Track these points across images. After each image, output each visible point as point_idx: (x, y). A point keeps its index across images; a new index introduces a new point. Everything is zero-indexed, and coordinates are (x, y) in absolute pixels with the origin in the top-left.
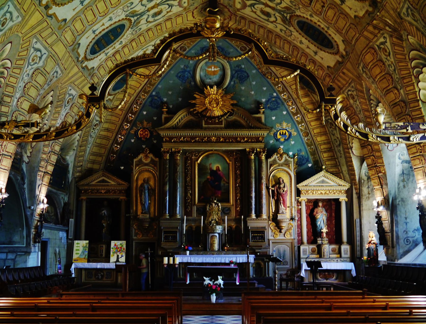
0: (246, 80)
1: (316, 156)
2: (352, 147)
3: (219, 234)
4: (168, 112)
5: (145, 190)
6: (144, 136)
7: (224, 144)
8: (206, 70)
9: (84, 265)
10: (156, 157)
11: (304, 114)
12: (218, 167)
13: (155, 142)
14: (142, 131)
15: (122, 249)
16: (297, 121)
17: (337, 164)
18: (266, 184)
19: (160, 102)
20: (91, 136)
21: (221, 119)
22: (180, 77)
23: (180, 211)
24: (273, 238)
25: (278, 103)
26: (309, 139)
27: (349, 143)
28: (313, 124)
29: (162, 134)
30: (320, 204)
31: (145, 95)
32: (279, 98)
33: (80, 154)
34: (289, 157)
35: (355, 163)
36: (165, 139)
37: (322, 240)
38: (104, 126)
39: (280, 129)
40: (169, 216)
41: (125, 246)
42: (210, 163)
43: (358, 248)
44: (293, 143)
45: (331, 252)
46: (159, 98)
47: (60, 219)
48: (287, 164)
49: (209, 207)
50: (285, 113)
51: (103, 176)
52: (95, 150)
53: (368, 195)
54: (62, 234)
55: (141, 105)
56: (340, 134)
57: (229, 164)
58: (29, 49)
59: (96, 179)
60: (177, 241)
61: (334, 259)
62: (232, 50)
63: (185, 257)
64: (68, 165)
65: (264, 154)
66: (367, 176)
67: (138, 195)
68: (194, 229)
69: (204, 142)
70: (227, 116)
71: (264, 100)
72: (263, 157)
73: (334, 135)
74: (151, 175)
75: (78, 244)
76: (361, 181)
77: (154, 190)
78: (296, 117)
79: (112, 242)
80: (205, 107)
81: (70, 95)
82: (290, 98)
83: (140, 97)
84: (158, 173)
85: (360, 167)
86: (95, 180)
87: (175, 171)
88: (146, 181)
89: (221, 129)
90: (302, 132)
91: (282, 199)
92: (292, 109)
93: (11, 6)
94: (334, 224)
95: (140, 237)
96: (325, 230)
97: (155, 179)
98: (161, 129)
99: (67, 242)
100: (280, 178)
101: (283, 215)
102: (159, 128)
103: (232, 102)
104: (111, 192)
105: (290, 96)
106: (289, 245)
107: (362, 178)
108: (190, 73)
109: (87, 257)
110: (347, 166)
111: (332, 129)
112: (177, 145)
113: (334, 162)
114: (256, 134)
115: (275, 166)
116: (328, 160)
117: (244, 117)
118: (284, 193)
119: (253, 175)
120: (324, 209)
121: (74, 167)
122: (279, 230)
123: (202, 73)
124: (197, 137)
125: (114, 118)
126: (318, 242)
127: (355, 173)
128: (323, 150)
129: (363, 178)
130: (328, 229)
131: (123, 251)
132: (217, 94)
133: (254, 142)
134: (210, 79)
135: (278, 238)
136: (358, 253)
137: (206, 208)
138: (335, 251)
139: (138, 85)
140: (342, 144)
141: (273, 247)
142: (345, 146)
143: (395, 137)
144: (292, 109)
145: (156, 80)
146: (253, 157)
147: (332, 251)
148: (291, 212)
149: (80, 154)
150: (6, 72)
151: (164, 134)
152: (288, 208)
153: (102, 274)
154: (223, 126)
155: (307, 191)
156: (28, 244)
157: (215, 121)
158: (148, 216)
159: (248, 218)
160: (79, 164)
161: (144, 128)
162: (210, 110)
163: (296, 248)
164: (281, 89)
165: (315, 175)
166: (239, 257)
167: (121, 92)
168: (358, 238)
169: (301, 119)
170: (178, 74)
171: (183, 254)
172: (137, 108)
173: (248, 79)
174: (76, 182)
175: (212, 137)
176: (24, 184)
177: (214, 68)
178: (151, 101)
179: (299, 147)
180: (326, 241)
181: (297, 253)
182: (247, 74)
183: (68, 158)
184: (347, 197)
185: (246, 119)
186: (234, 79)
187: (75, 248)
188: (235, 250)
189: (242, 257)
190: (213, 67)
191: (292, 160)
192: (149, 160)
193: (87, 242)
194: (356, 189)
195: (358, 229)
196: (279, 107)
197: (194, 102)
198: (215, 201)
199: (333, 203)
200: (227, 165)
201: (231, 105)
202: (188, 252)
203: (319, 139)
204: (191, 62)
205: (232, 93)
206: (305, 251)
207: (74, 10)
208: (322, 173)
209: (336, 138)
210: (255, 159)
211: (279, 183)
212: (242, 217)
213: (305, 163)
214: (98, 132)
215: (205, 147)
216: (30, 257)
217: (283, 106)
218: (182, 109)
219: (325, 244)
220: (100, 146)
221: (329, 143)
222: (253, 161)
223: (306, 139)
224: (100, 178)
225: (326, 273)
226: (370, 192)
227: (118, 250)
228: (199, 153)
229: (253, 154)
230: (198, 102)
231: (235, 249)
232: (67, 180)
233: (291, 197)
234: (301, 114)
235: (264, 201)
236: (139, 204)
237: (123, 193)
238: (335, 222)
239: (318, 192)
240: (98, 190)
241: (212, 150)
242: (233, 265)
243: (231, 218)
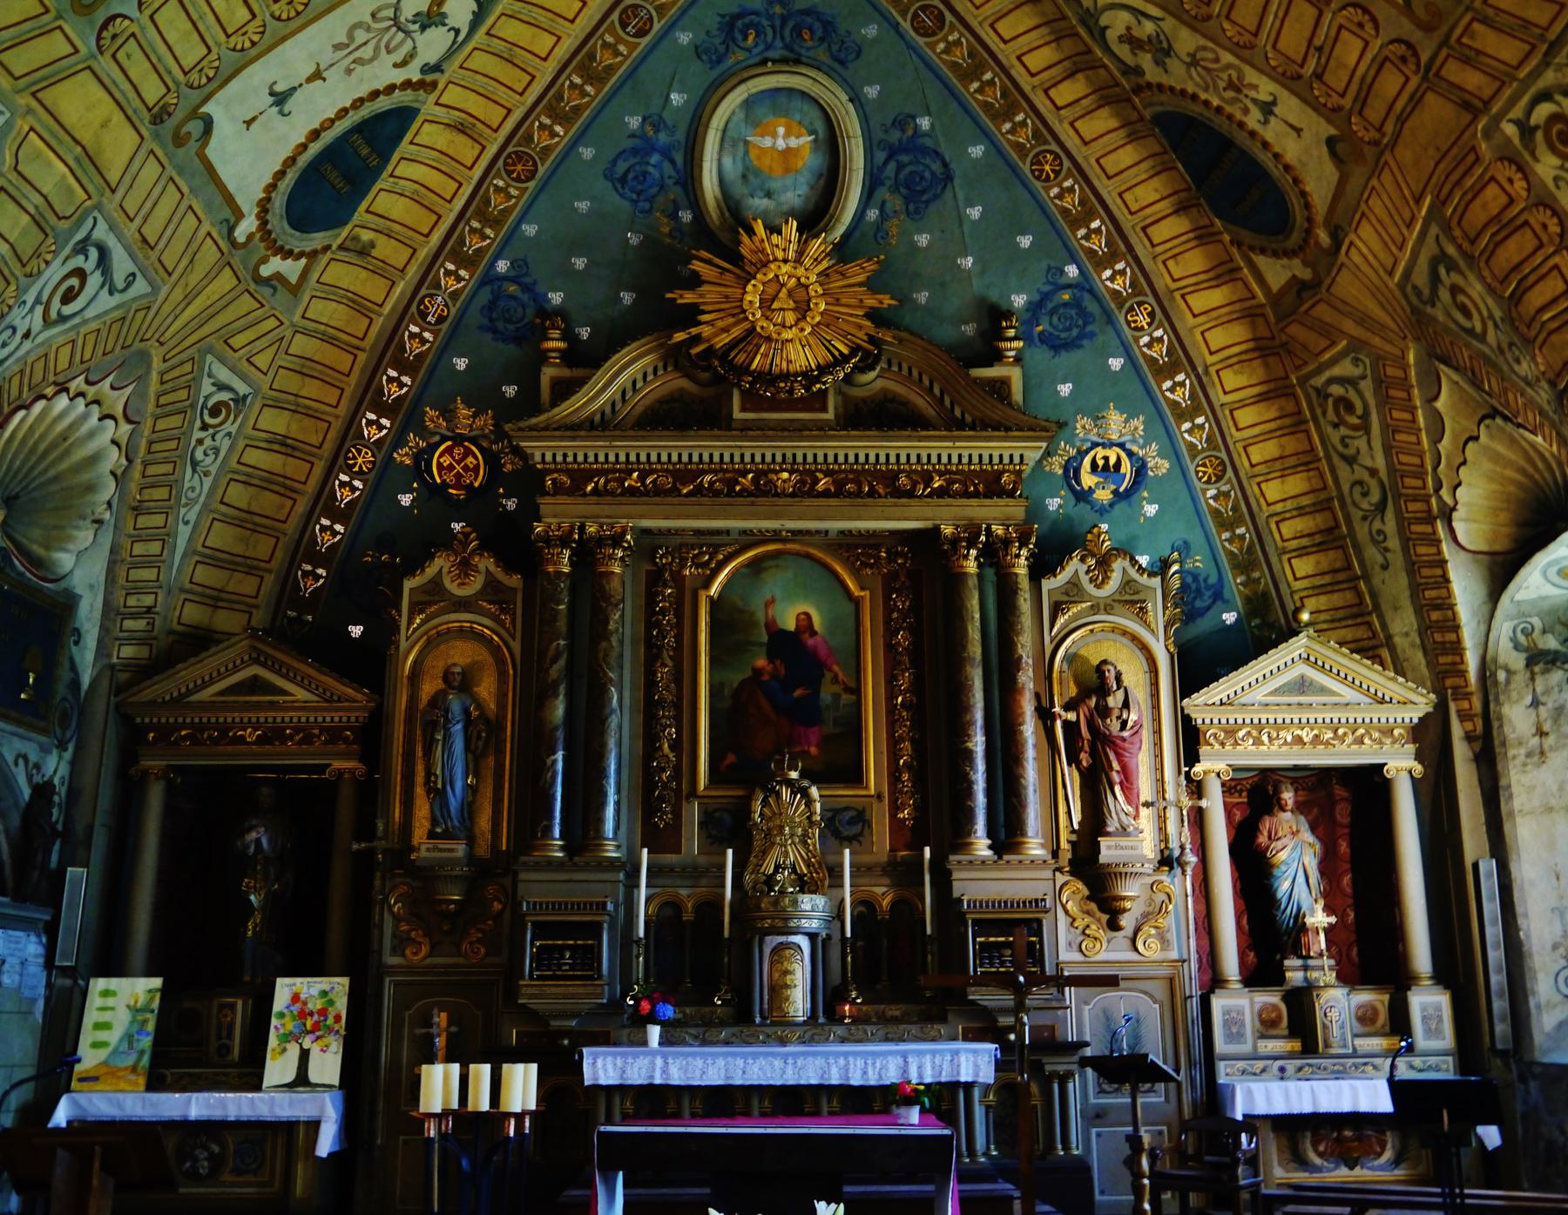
0: (936, 197)
1: (1256, 575)
2: (1454, 509)
3: (812, 936)
4: (568, 358)
5: (447, 721)
6: (458, 476)
7: (833, 502)
8: (746, 143)
9: (120, 1106)
10: (509, 568)
11: (1206, 368)
12: (807, 615)
13: (511, 504)
14: (449, 451)
15: (330, 1021)
16: (1174, 405)
17: (1361, 602)
18: (1037, 696)
19: (530, 312)
20: (195, 464)
21: (817, 380)
22: (623, 180)
23: (623, 828)
25: (1086, 317)
26: (1227, 495)
27: (1438, 486)
28: (1246, 416)
29: (538, 458)
30: (1288, 796)
31: (462, 273)
32: (1092, 292)
33: (139, 549)
34: (1141, 570)
35: (1465, 588)
36: (554, 480)
37: (1306, 968)
38: (262, 424)
39: (1095, 445)
40: (562, 848)
41: (341, 1005)
42: (768, 597)
43: (1500, 1005)
44: (1151, 510)
45: (1358, 1028)
46: (527, 288)
47: (8, 870)
48: (1131, 599)
49: (765, 803)
50: (1116, 363)
51: (256, 661)
52: (222, 537)
53: (1536, 740)
55: (445, 327)
56: (1387, 449)
57: (857, 602)
59: (221, 677)
60: (600, 977)
61: (1378, 1061)
62: (871, 31)
63: (636, 1056)
64: (69, 602)
65: (1024, 552)
66: (1526, 650)
67: (419, 753)
68: (688, 916)
69: (739, 494)
70: (848, 368)
71: (1019, 301)
72: (1021, 568)
73: (1351, 461)
74: (482, 654)
75: (106, 993)
76: (1494, 675)
77: (495, 727)
78: (1168, 384)
79: (280, 982)
80: (746, 325)
82: (1142, 293)
83: (438, 286)
84: (516, 646)
85: (1486, 609)
86: (212, 681)
87: (599, 630)
88: (462, 682)
89: (820, 429)
90: (1193, 457)
91: (1116, 766)
92: (1152, 342)
94: (1349, 890)
95: (419, 954)
96: (1319, 918)
97: (502, 675)
98: (531, 428)
99: (49, 985)
100: (1105, 662)
101: (1123, 841)
102: (522, 424)
103: (871, 302)
104: (291, 737)
105: (1143, 281)
106: (1160, 990)
107: (1495, 660)
108: (672, 162)
109: (146, 1060)
110: (1419, 610)
111: (1343, 431)
112: (607, 510)
113: (1349, 597)
114: (986, 459)
115: (1075, 610)
116: (1319, 590)
117: (926, 382)
118: (1126, 734)
119: (975, 650)
120: (1302, 818)
121: (109, 610)
122: (1105, 917)
123: (727, 161)
124: (705, 472)
125: (312, 389)
126: (1288, 974)
127: (1459, 641)
128: (1294, 544)
129: (1501, 660)
130: (1328, 909)
131: (330, 1030)
132: (798, 261)
133: (976, 495)
134: (769, 195)
135: (1099, 958)
136: (1502, 1029)
137: (748, 812)
138: (1373, 1020)
139: (424, 221)
140: (1398, 496)
142: (1412, 506)
144: (1149, 345)
145: (510, 197)
146: (971, 566)
147: (1362, 1019)
148: (1162, 829)
149: (139, 549)
151: (549, 458)
152: (1144, 812)
153: (216, 1148)
154: (830, 415)
155: (1231, 732)
157: (791, 391)
158: (460, 849)
159: (952, 858)
160: (132, 601)
161: (458, 440)
162: (769, 339)
163: (1194, 1004)
164: (1098, 244)
165: (1246, 663)
166: (920, 1053)
167: (341, 247)
168: (1496, 955)
169: (1193, 396)
170: (614, 162)
171: (632, 1044)
172: (423, 341)
173: (948, 195)
174: (119, 689)
175: (777, 472)
177: (787, 135)
178: (491, 306)
179: (1182, 530)
180: (1324, 972)
181: (1198, 1031)
182: (945, 165)
184: (1419, 757)
185: (937, 391)
186: (882, 193)
187: (91, 1016)
188: (895, 1021)
189: (934, 1053)
190: (781, 130)
191: (1156, 581)
192: (476, 584)
193: (157, 982)
194: (1464, 716)
195: (1492, 908)
196: (1092, 335)
197: (689, 297)
198: (794, 775)
199: (1340, 792)
200: (850, 608)
201: (867, 316)
202: (654, 1032)
203: (1273, 490)
204: (675, 98)
205: (868, 261)
206: (1232, 1022)
208: (1298, 645)
209: (1366, 476)
210: (980, 576)
211: (1103, 690)
212: (927, 851)
213: (1208, 608)
214: (231, 449)
215: (744, 517)
217: (1109, 329)
218: (635, 339)
219: (1326, 986)
220: (245, 521)
221: (1323, 506)
222: (972, 582)
223: (1211, 492)
224: (236, 669)
225: (1348, 1133)
226: (1546, 728)
227: (309, 1023)
228: (715, 546)
229: (973, 552)
230: (710, 298)
231: (895, 1011)
232: (65, 675)
233: (1159, 756)
234: (1194, 368)
235: (1031, 773)
236: (420, 790)
237: (346, 740)
238: (1354, 881)
239: (1282, 734)
240: (224, 729)
241: (776, 536)
242: (914, 1115)
243: (866, 859)
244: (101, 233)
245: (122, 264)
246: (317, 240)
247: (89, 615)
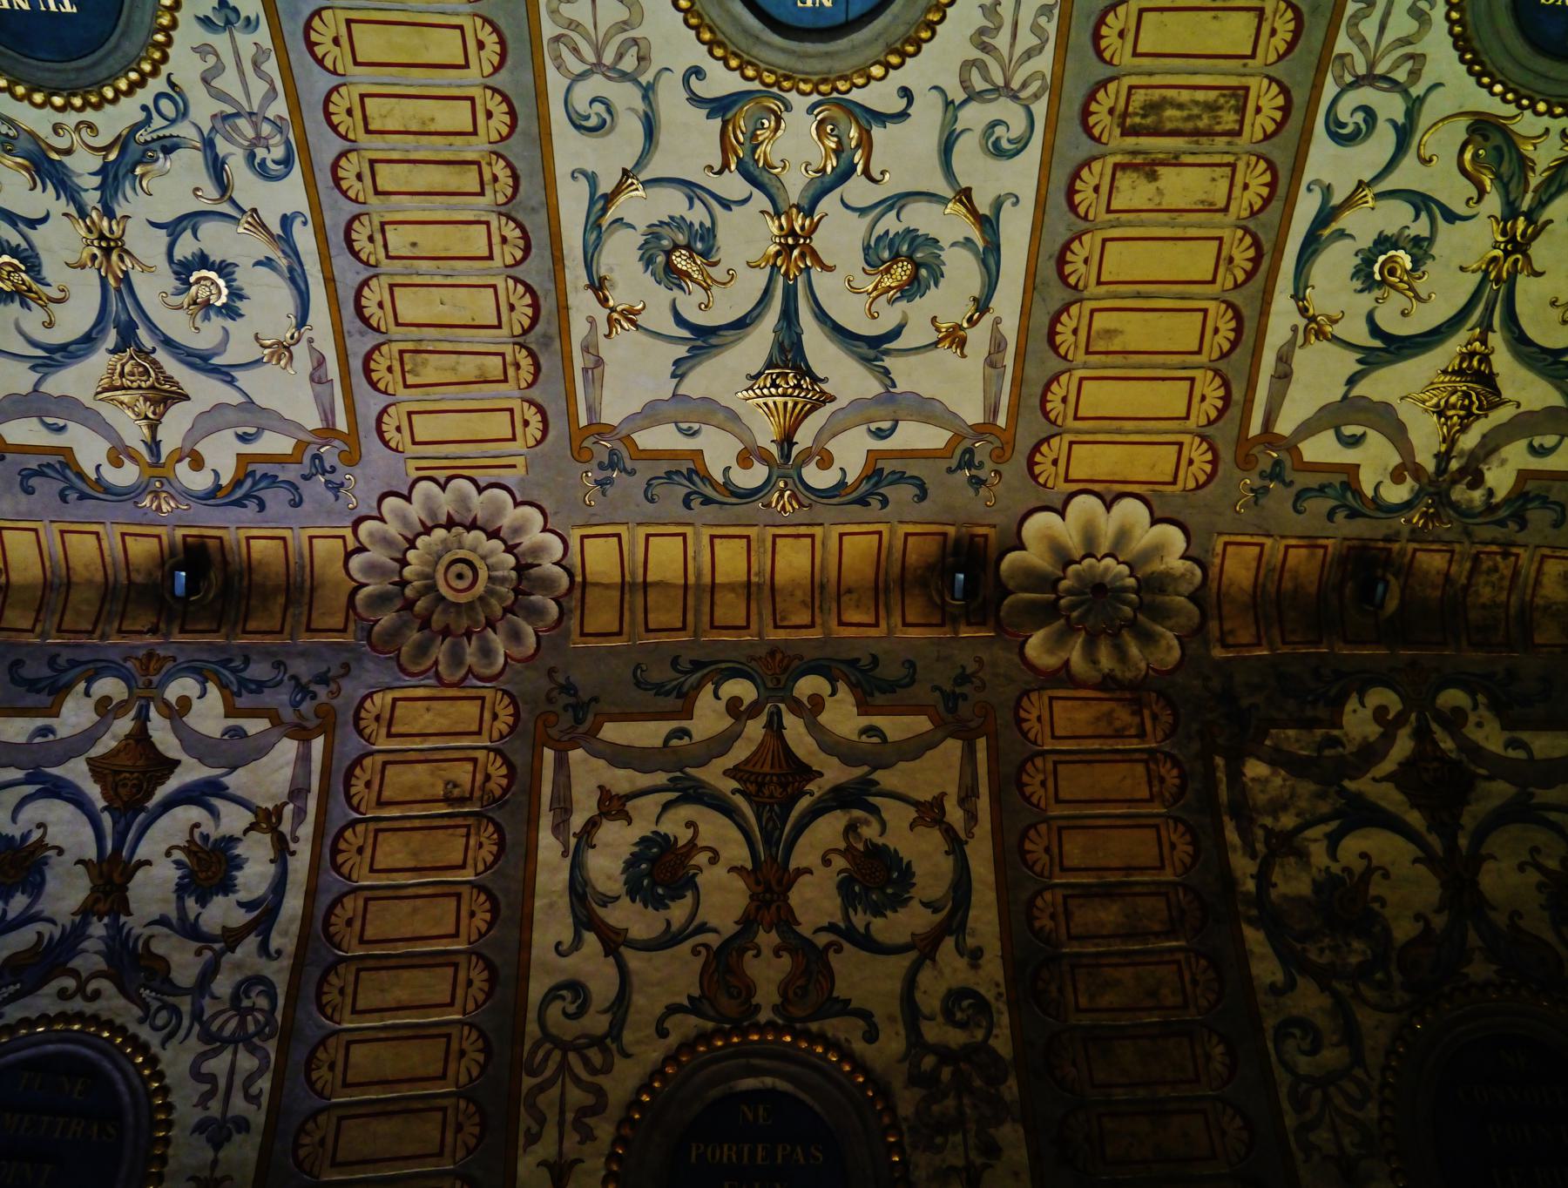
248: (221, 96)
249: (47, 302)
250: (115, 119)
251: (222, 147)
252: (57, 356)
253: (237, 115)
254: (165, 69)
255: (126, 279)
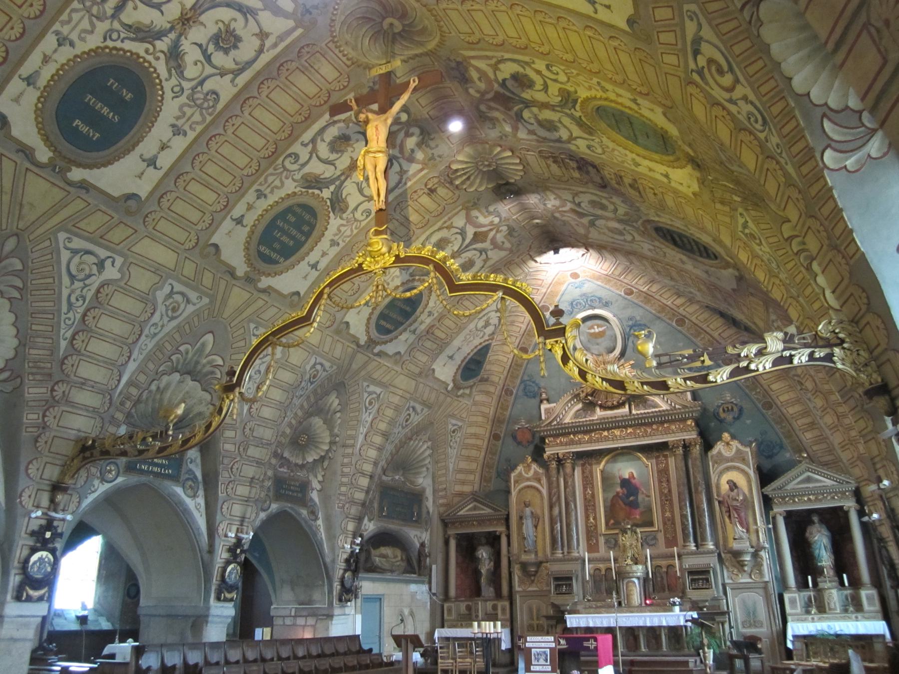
19: (536, 389)
24: (730, 581)
44: (748, 422)
54: (425, 588)
58: (247, 338)
81: (370, 393)
93: (175, 284)
121: (435, 491)
135: (742, 581)
141: (734, 597)
143: (679, 380)
149: (440, 473)
150: (218, 372)
156: (331, 604)
176: (317, 519)
178: (525, 389)
183: (420, 481)
189: (665, 616)
203: (791, 410)
207: (305, 277)
216: (334, 622)
232: (424, 511)
244: (412, 404)
245: (419, 407)
246: (471, 382)
247: (429, 493)
248: (93, 25)
249: (228, 26)
250: (139, 48)
251: (110, 12)
252: (245, 10)
253: (93, 15)
254: (102, 45)
255: (193, 8)
